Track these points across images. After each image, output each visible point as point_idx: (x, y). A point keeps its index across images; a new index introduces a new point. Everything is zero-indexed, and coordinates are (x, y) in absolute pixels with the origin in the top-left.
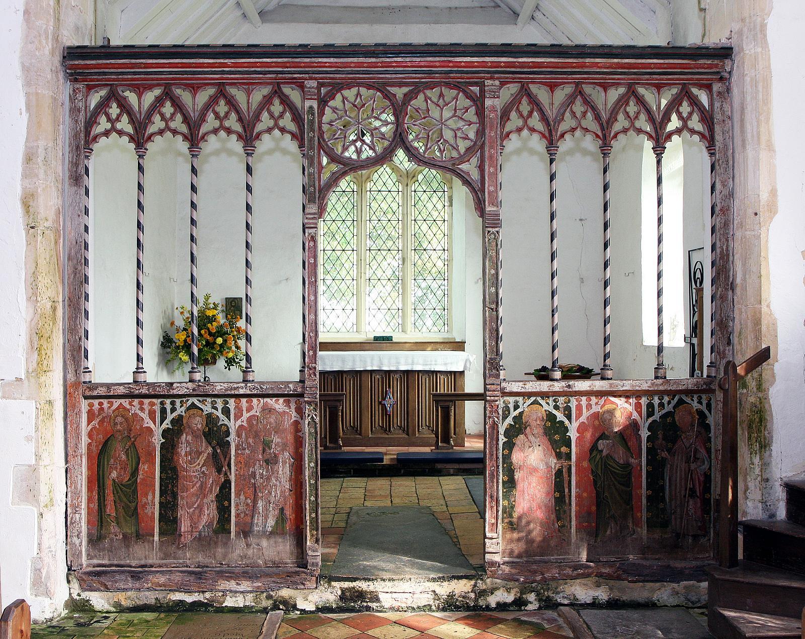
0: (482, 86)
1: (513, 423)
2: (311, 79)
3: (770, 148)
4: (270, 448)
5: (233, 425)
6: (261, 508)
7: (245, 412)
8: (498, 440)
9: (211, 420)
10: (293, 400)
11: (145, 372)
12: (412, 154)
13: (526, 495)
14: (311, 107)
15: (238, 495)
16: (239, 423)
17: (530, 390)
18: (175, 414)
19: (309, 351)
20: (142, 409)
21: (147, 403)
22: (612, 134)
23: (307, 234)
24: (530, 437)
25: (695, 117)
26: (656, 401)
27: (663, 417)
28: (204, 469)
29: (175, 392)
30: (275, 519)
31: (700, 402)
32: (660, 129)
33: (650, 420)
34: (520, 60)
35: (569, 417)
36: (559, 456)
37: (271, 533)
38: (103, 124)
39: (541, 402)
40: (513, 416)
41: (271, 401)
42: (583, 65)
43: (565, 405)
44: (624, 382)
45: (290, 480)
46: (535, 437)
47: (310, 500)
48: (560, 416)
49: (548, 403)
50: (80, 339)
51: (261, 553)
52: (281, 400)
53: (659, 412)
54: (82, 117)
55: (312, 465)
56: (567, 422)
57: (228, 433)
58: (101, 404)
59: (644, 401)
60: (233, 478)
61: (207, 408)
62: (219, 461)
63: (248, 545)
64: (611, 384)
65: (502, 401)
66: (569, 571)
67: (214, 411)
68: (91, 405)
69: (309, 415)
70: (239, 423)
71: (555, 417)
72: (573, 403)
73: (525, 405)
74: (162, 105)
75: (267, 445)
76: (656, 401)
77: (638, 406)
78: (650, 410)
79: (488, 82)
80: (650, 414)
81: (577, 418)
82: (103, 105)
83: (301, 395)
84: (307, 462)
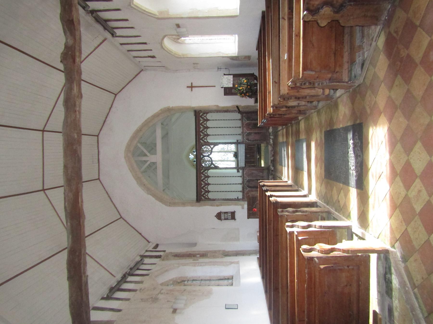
0: (201, 145)
3: (209, 106)
5: (248, 179)
10: (244, 170)
12: (211, 154)
35: (247, 132)
36: (252, 134)
38: (207, 197)
48: (246, 134)
52: (244, 172)
57: (249, 179)
62: (253, 180)
66: (268, 132)
73: (245, 138)
80: (246, 121)
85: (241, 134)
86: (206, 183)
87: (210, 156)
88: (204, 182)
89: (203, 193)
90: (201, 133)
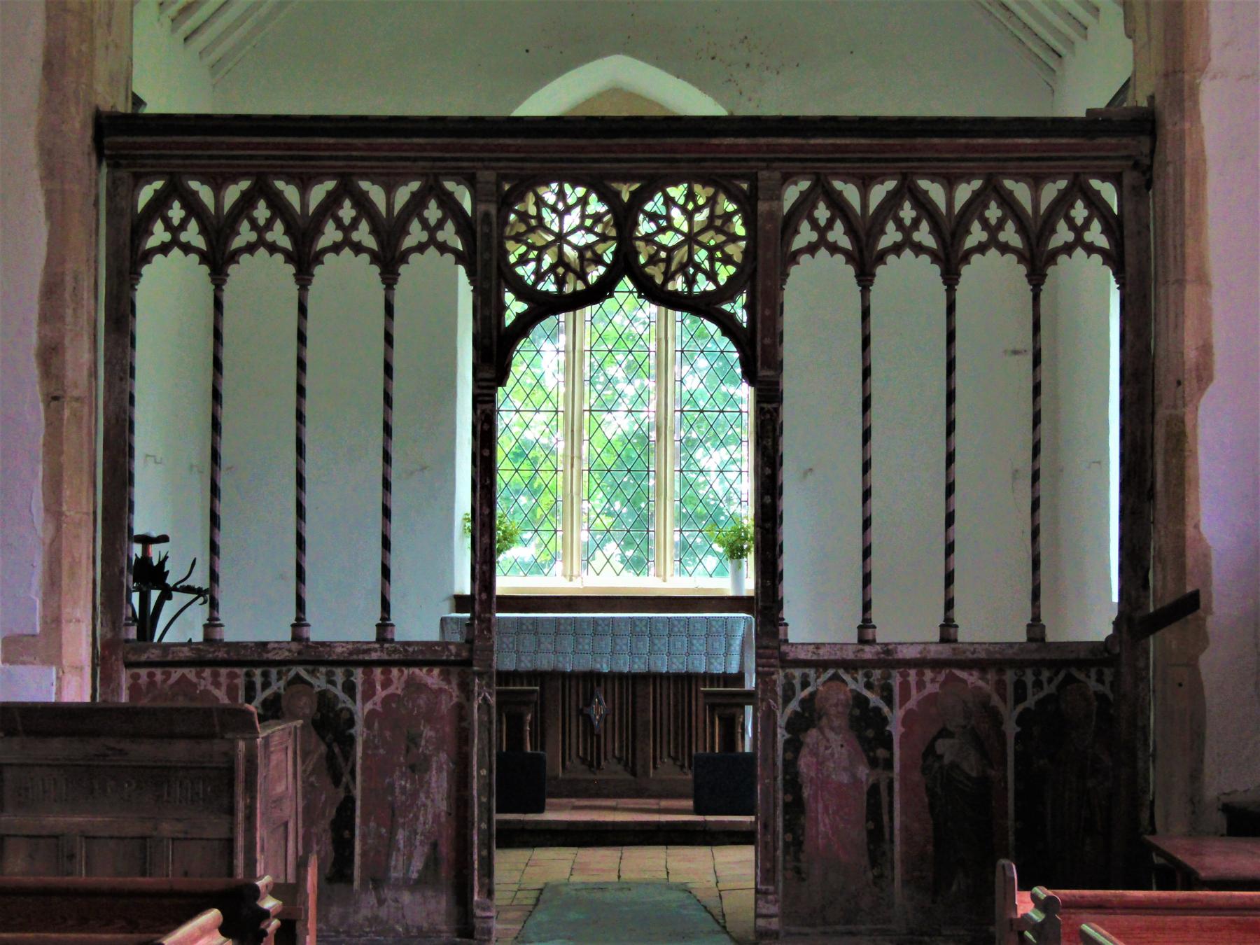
0: (753, 180)
1: (799, 709)
2: (487, 168)
3: (1203, 280)
4: (417, 745)
5: (360, 709)
6: (402, 842)
7: (378, 687)
8: (775, 735)
9: (325, 701)
11: (221, 625)
13: (821, 825)
14: (487, 215)
15: (365, 822)
16: (369, 706)
17: (826, 658)
18: (268, 692)
19: (480, 594)
20: (217, 685)
21: (225, 674)
22: (960, 254)
23: (479, 412)
24: (827, 731)
25: (1096, 226)
26: (1029, 678)
27: (1040, 703)
28: (313, 779)
29: (270, 656)
30: (423, 859)
31: (1100, 680)
32: (1038, 245)
33: (1020, 708)
34: (812, 141)
35: (889, 701)
36: (873, 763)
37: (417, 882)
38: (159, 235)
39: (847, 677)
40: (800, 698)
41: (421, 673)
42: (913, 149)
43: (883, 682)
44: (977, 646)
45: (449, 797)
46: (836, 733)
47: (479, 828)
48: (874, 699)
49: (855, 680)
50: (122, 572)
51: (400, 916)
53: (1034, 695)
54: (126, 224)
55: (484, 772)
56: (886, 709)
57: (351, 722)
58: (151, 675)
59: (1010, 676)
60: (358, 793)
61: (320, 683)
63: (381, 902)
64: (954, 649)
65: (781, 673)
67: (329, 686)
68: (136, 677)
69: (479, 695)
70: (369, 706)
71: (867, 700)
72: (896, 681)
73: (818, 681)
74: (254, 206)
75: (413, 740)
76: (1029, 678)
77: (1000, 686)
78: (1020, 691)
79: (763, 174)
80: (1020, 696)
81: (902, 704)
82: (158, 206)
83: (468, 663)
84: (475, 768)
85: (872, 642)
86: (318, 231)
87: (626, 284)
88: (330, 205)
89: (205, 193)
90: (891, 185)
